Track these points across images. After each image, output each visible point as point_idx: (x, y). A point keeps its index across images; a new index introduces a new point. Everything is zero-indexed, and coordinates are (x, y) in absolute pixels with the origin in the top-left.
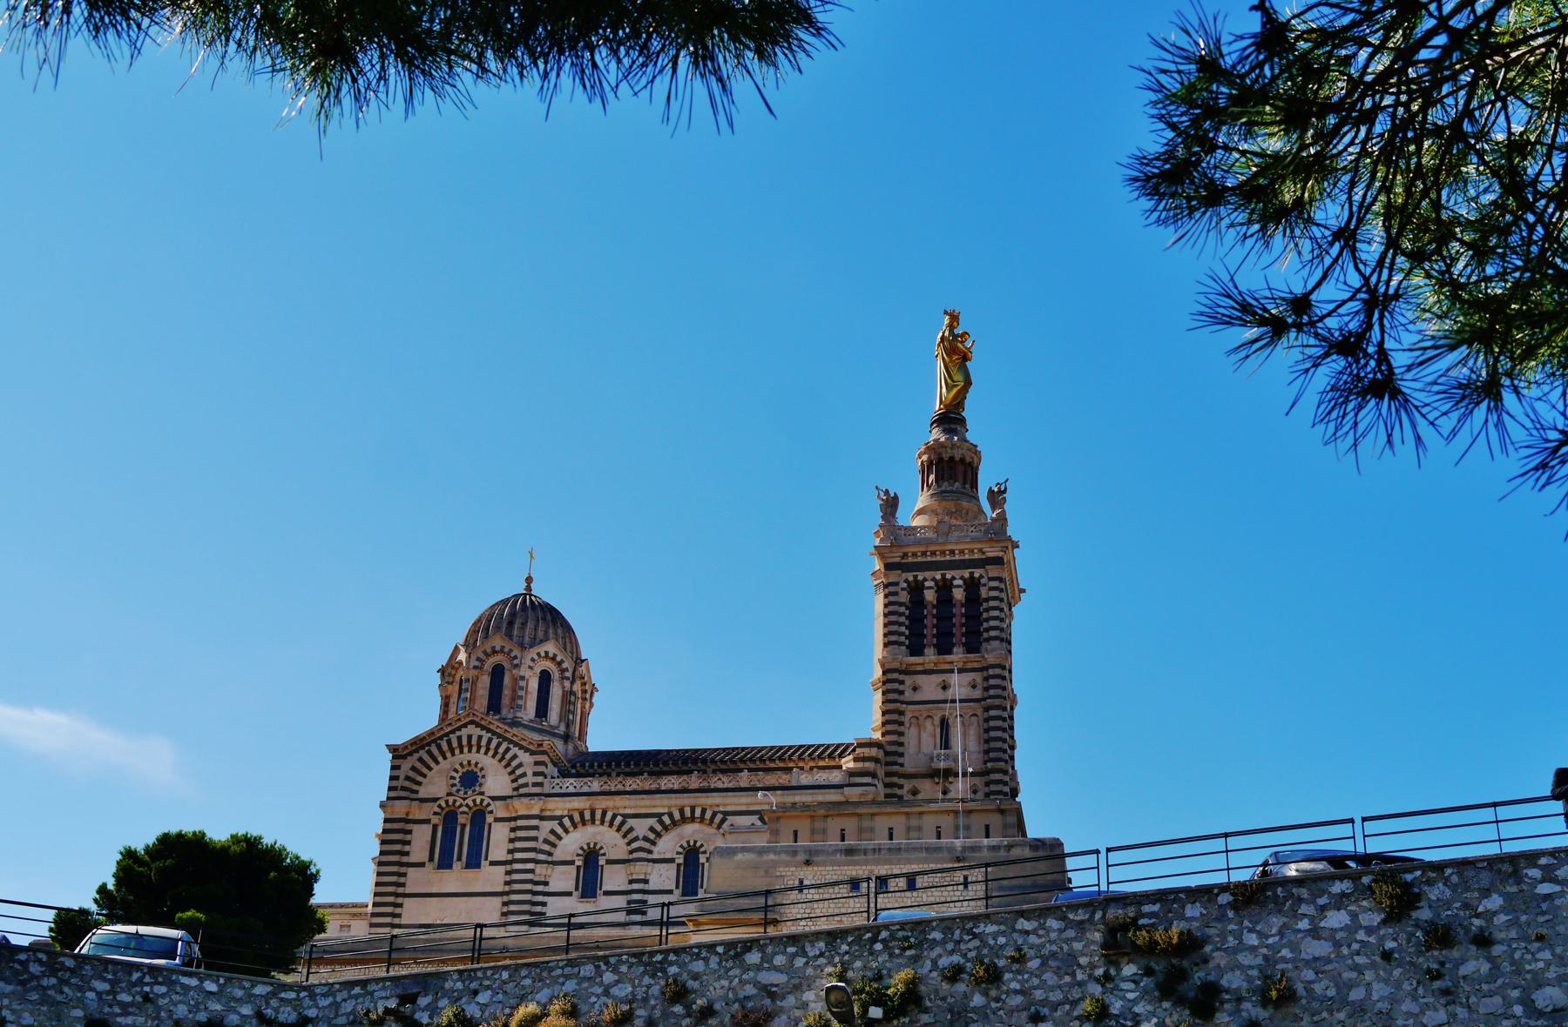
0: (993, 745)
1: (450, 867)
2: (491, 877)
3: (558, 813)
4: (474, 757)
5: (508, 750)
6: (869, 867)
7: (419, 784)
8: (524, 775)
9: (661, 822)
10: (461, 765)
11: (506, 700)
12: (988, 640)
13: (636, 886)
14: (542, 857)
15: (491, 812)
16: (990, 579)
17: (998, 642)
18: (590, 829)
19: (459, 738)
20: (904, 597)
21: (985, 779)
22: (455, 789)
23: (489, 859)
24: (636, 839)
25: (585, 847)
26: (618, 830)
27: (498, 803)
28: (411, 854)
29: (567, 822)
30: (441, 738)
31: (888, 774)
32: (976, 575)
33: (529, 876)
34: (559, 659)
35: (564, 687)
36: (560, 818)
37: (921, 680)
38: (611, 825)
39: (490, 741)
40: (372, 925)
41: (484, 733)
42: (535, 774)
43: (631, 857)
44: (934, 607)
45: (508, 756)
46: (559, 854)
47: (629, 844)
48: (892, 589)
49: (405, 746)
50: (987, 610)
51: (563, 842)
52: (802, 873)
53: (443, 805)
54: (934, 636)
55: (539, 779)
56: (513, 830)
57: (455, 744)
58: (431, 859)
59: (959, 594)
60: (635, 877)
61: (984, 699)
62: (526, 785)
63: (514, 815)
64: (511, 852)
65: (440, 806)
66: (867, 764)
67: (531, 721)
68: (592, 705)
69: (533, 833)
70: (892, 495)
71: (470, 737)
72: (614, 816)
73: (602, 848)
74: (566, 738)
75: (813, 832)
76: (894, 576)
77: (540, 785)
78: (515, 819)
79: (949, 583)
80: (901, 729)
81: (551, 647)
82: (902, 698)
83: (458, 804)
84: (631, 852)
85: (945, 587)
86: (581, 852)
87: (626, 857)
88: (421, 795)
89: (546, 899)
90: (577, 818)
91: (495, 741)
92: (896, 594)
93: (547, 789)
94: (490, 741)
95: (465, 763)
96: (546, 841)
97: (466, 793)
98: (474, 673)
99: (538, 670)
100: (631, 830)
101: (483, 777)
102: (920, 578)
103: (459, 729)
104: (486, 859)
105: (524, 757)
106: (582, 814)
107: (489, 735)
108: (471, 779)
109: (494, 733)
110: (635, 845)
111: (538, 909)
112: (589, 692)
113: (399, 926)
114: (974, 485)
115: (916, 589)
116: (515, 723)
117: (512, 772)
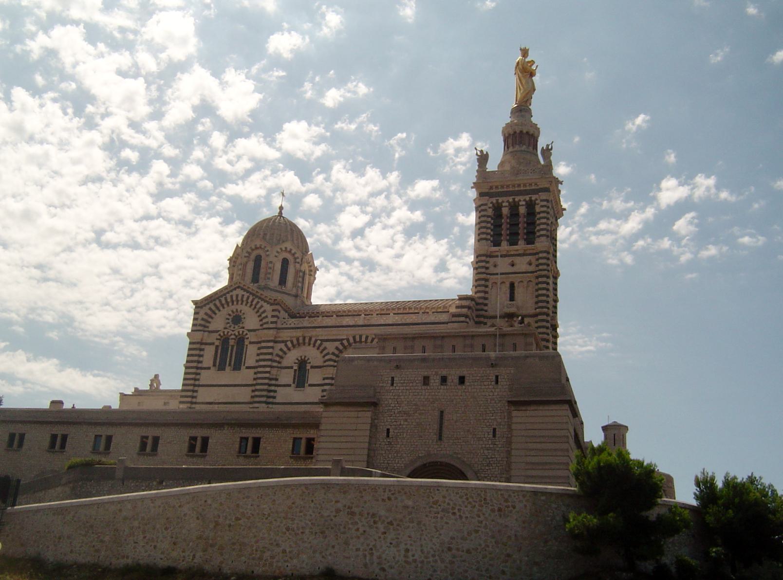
0: (541, 298)
1: (224, 369)
2: (245, 376)
3: (285, 339)
4: (240, 307)
5: (258, 302)
6: (436, 370)
7: (209, 322)
8: (267, 317)
9: (342, 344)
10: (233, 311)
11: (262, 275)
12: (539, 237)
13: (327, 381)
14: (275, 364)
16: (542, 201)
17: (545, 238)
18: (303, 348)
19: (232, 296)
20: (490, 212)
21: (535, 319)
22: (228, 325)
23: (246, 365)
24: (328, 354)
25: (300, 359)
26: (318, 349)
28: (203, 363)
29: (289, 344)
30: (221, 296)
32: (533, 199)
33: (267, 375)
34: (293, 252)
36: (285, 342)
37: (499, 260)
38: (314, 346)
39: (248, 298)
40: (181, 402)
41: (245, 293)
42: (273, 316)
43: (325, 364)
44: (508, 218)
45: (258, 306)
46: (285, 363)
47: (324, 357)
48: (483, 208)
50: (539, 219)
51: (287, 355)
52: (393, 373)
53: (222, 334)
54: (507, 235)
55: (275, 319)
57: (229, 300)
58: (214, 365)
59: (522, 210)
60: (326, 376)
61: (536, 272)
62: (267, 323)
63: (260, 340)
64: (257, 361)
65: (220, 335)
66: (463, 310)
67: (276, 287)
68: (315, 279)
69: (270, 350)
70: (485, 153)
71: (237, 296)
72: (316, 341)
73: (308, 359)
74: (296, 296)
75: (406, 348)
76: (485, 200)
77: (276, 322)
78: (260, 342)
79: (517, 204)
80: (487, 289)
81: (288, 245)
82: (488, 271)
83: (229, 334)
84: (325, 362)
85: (514, 207)
86: (297, 361)
87: (321, 364)
88: (210, 329)
89: (276, 388)
90: (295, 342)
92: (485, 210)
93: (279, 326)
94: (248, 298)
95: (235, 310)
96: (278, 355)
97: (234, 328)
98: (245, 259)
99: (281, 257)
100: (325, 348)
101: (244, 318)
102: (500, 201)
104: (244, 365)
105: (267, 307)
106: (298, 340)
107: (248, 294)
108: (237, 319)
109: (251, 293)
110: (327, 357)
111: (272, 394)
113: (196, 403)
114: (535, 147)
115: (497, 208)
116: (266, 288)
117: (260, 316)
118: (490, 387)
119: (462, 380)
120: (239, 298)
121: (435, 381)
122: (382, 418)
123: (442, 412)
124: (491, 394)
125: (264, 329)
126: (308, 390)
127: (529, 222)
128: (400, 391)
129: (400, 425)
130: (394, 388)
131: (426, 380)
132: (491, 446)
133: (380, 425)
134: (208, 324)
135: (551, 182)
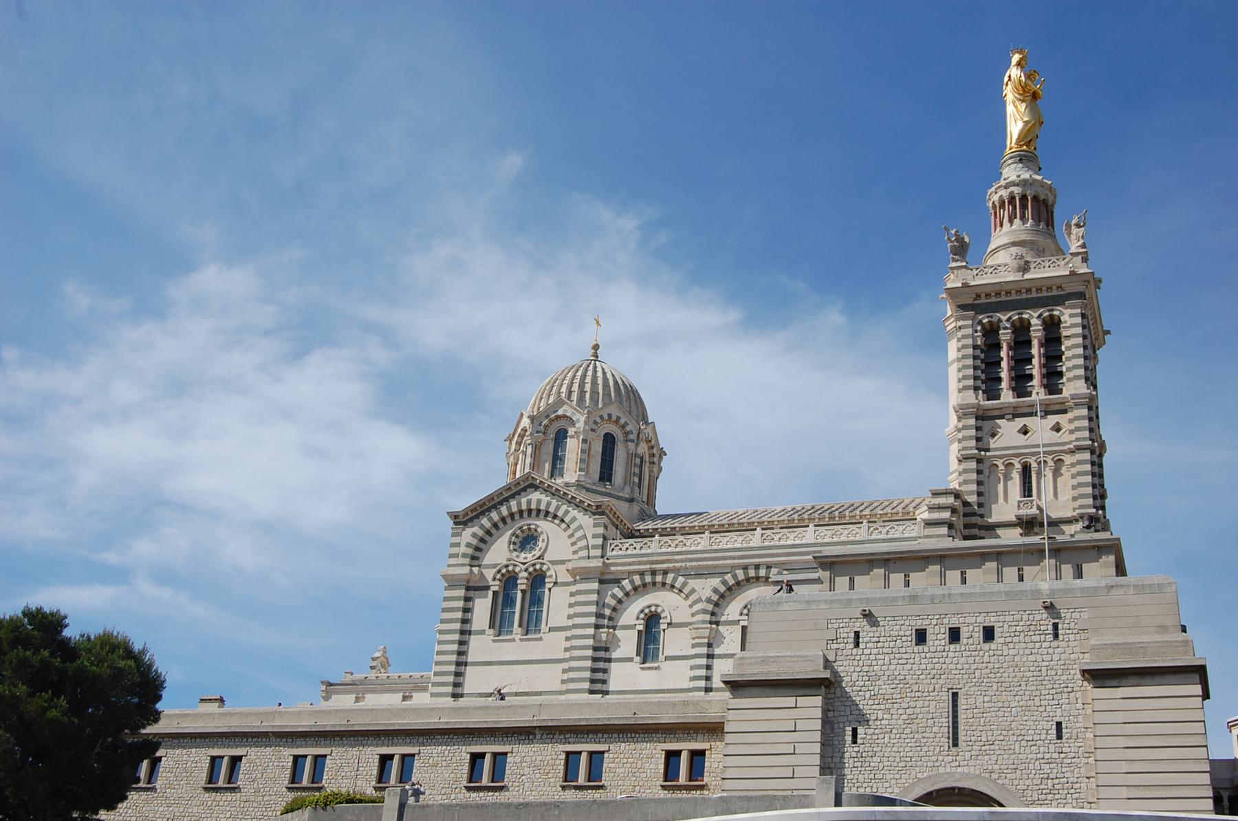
2: (551, 644)
24: (699, 600)
27: (558, 568)
31: (966, 526)
34: (622, 421)
35: (628, 450)
47: (691, 606)
49: (466, 512)
68: (660, 469)
79: (1026, 324)
84: (693, 615)
100: (693, 591)
112: (658, 456)
115: (991, 332)
118: (1045, 645)
119: (989, 634)
121: (940, 636)
122: (843, 708)
123: (955, 695)
124: (1048, 658)
125: (580, 558)
126: (667, 666)
127: (1051, 354)
128: (872, 657)
129: (876, 719)
130: (860, 652)
131: (921, 636)
132: (1055, 755)
133: (838, 723)
135: (1088, 281)
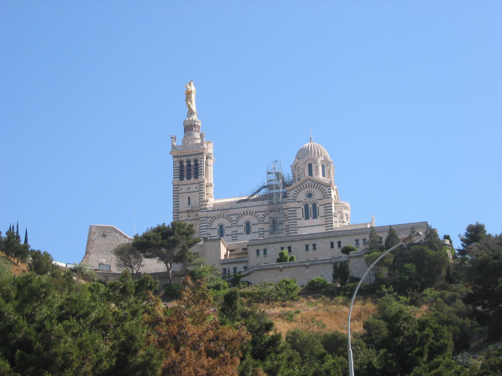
5: (320, 186)
8: (326, 193)
15: (318, 203)
23: (320, 215)
27: (319, 201)
30: (300, 185)
39: (315, 184)
56: (325, 207)
57: (305, 186)
58: (303, 217)
65: (303, 203)
78: (325, 204)
91: (316, 184)
94: (315, 184)
101: (314, 194)
103: (305, 182)
108: (310, 195)
120: (310, 185)
134: (296, 199)
